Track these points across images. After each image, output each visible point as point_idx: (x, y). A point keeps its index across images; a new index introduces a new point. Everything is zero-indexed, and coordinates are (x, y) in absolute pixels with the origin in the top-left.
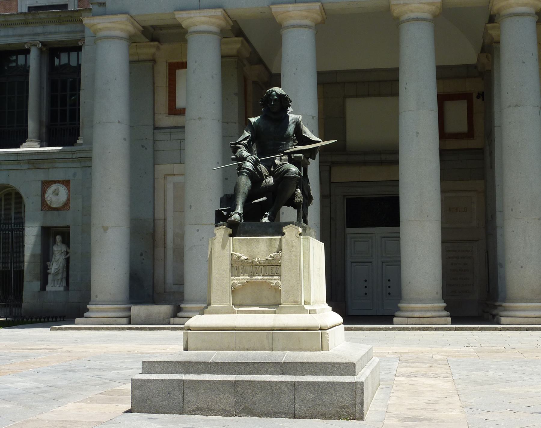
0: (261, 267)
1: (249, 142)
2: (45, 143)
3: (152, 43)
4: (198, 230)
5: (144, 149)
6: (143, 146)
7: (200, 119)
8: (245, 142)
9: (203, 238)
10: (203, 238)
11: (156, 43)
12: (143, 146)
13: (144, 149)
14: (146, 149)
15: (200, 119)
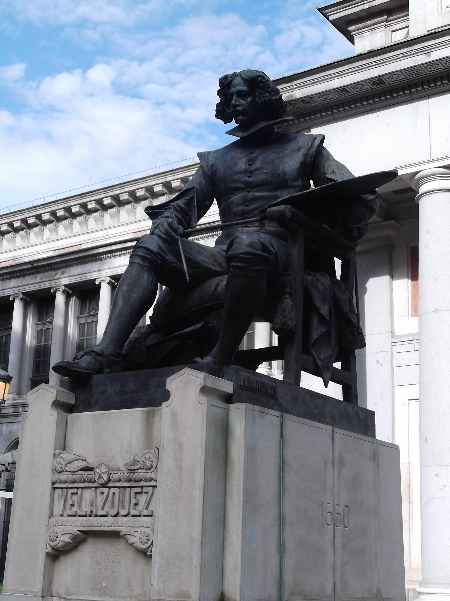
0: (112, 490)
1: (189, 203)
2: (276, 370)
3: (386, 223)
4: (437, 475)
5: (379, 365)
6: (378, 362)
7: (436, 311)
8: (180, 202)
9: (444, 486)
10: (444, 486)
11: (393, 222)
12: (378, 362)
13: (379, 365)
14: (382, 365)
15: (436, 311)
